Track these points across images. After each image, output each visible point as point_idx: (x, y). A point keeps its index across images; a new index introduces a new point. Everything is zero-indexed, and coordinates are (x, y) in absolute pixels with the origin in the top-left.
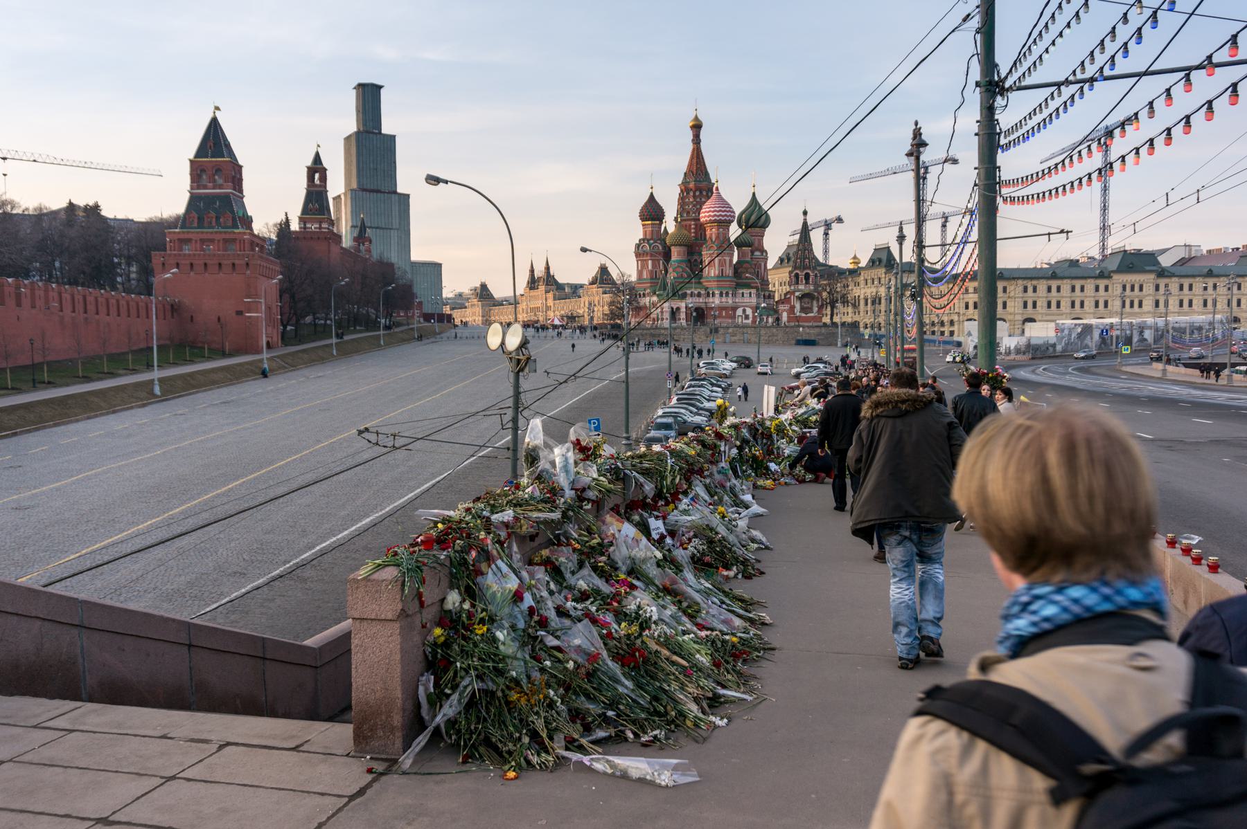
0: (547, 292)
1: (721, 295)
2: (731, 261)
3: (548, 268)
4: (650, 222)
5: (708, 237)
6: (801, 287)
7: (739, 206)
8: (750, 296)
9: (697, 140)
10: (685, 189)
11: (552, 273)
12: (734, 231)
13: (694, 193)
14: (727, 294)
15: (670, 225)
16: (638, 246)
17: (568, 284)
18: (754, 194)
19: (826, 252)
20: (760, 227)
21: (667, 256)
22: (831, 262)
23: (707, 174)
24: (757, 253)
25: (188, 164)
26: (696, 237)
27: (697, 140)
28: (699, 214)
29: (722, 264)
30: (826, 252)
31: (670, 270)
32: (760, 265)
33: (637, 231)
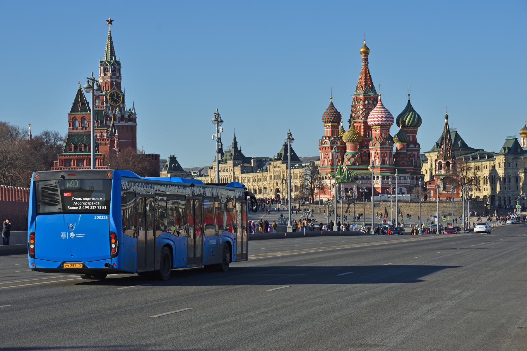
0: (235, 165)
1: (383, 178)
2: (391, 153)
3: (235, 143)
4: (330, 124)
5: (373, 135)
6: (443, 172)
8: (405, 179)
11: (239, 148)
13: (364, 102)
14: (388, 177)
17: (254, 158)
18: (409, 101)
20: (414, 127)
21: (343, 149)
24: (412, 146)
25: (68, 115)
26: (365, 135)
28: (367, 119)
31: (346, 160)
32: (414, 155)
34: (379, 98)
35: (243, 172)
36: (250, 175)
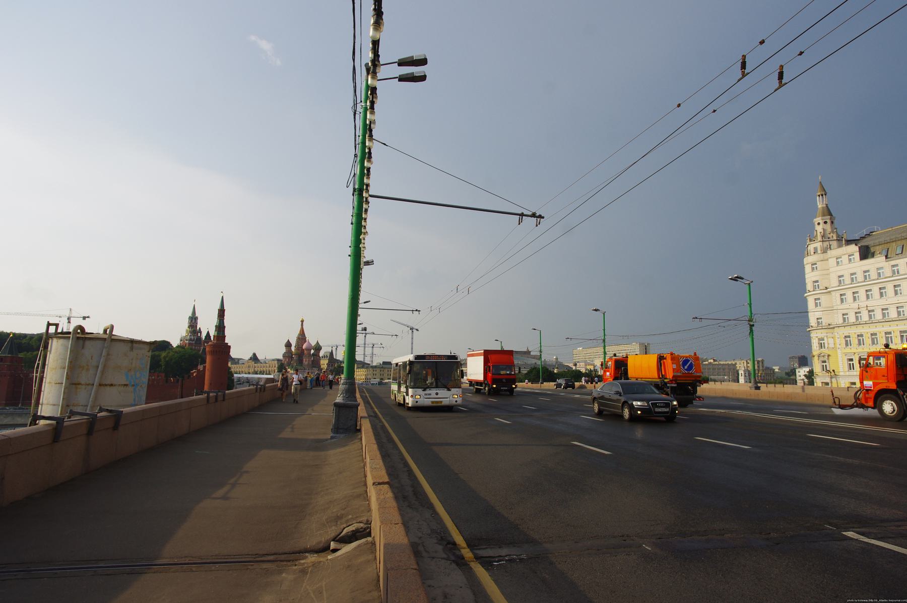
7: (313, 344)
9: (302, 325)
10: (298, 339)
12: (312, 351)
15: (293, 349)
16: (283, 354)
19: (336, 355)
22: (337, 359)
23: (305, 335)
27: (302, 325)
29: (309, 361)
30: (336, 355)
33: (284, 350)
34: (307, 339)
35: (232, 364)
36: (235, 365)
